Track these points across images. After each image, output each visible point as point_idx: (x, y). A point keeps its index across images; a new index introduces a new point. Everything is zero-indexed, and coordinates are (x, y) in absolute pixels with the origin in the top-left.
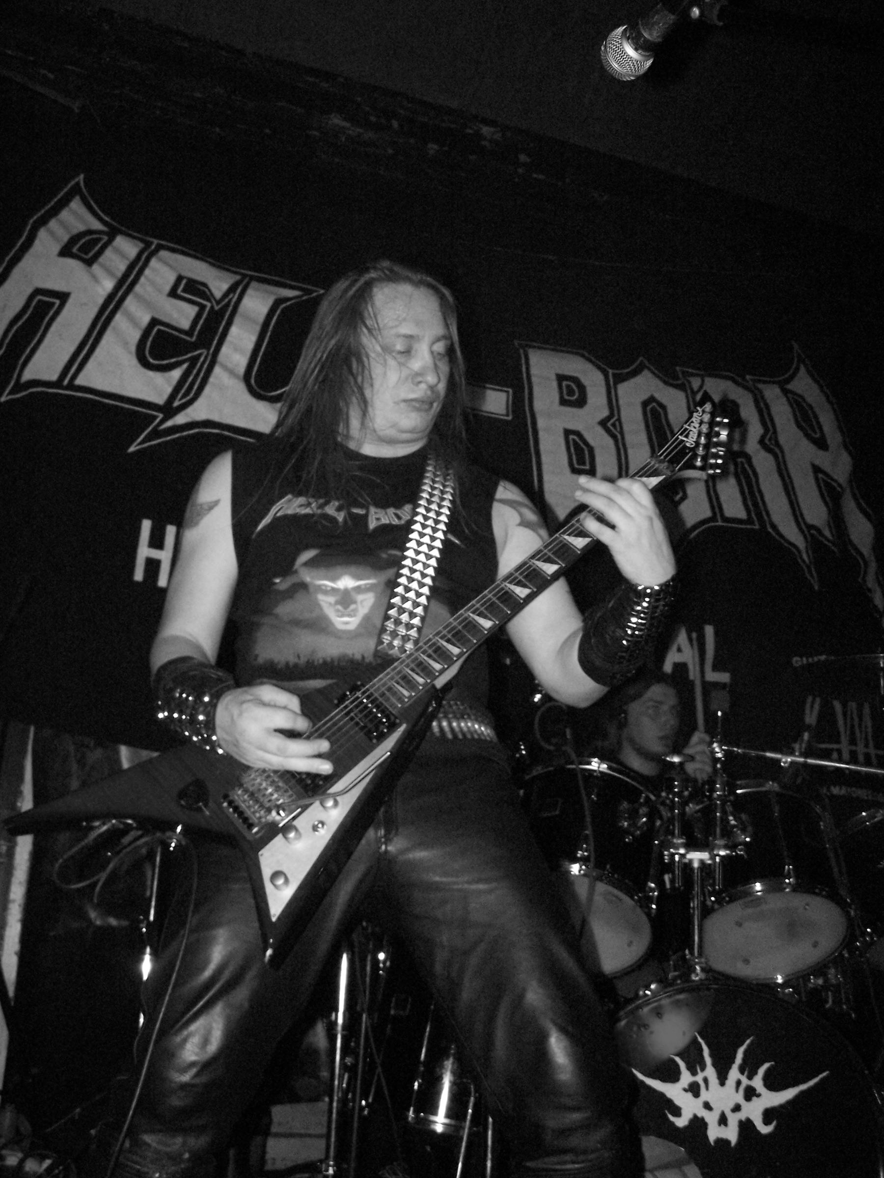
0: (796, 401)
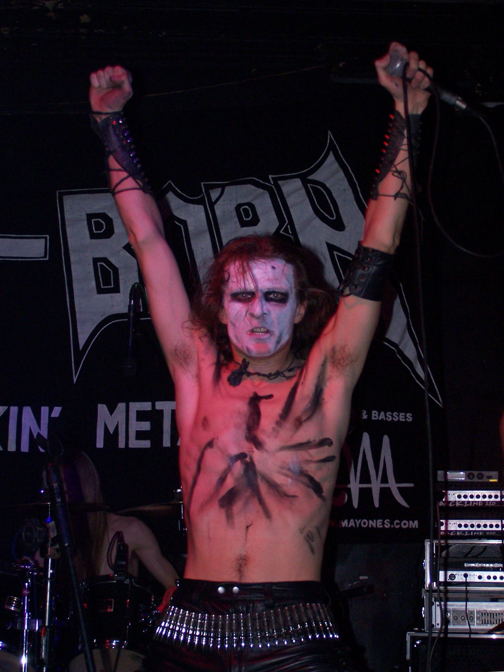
0: (316, 190)
